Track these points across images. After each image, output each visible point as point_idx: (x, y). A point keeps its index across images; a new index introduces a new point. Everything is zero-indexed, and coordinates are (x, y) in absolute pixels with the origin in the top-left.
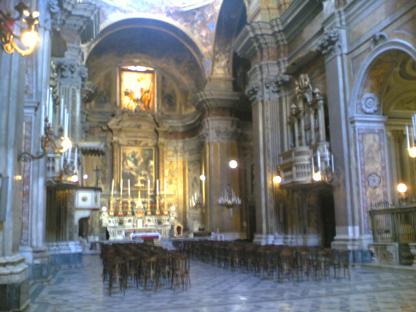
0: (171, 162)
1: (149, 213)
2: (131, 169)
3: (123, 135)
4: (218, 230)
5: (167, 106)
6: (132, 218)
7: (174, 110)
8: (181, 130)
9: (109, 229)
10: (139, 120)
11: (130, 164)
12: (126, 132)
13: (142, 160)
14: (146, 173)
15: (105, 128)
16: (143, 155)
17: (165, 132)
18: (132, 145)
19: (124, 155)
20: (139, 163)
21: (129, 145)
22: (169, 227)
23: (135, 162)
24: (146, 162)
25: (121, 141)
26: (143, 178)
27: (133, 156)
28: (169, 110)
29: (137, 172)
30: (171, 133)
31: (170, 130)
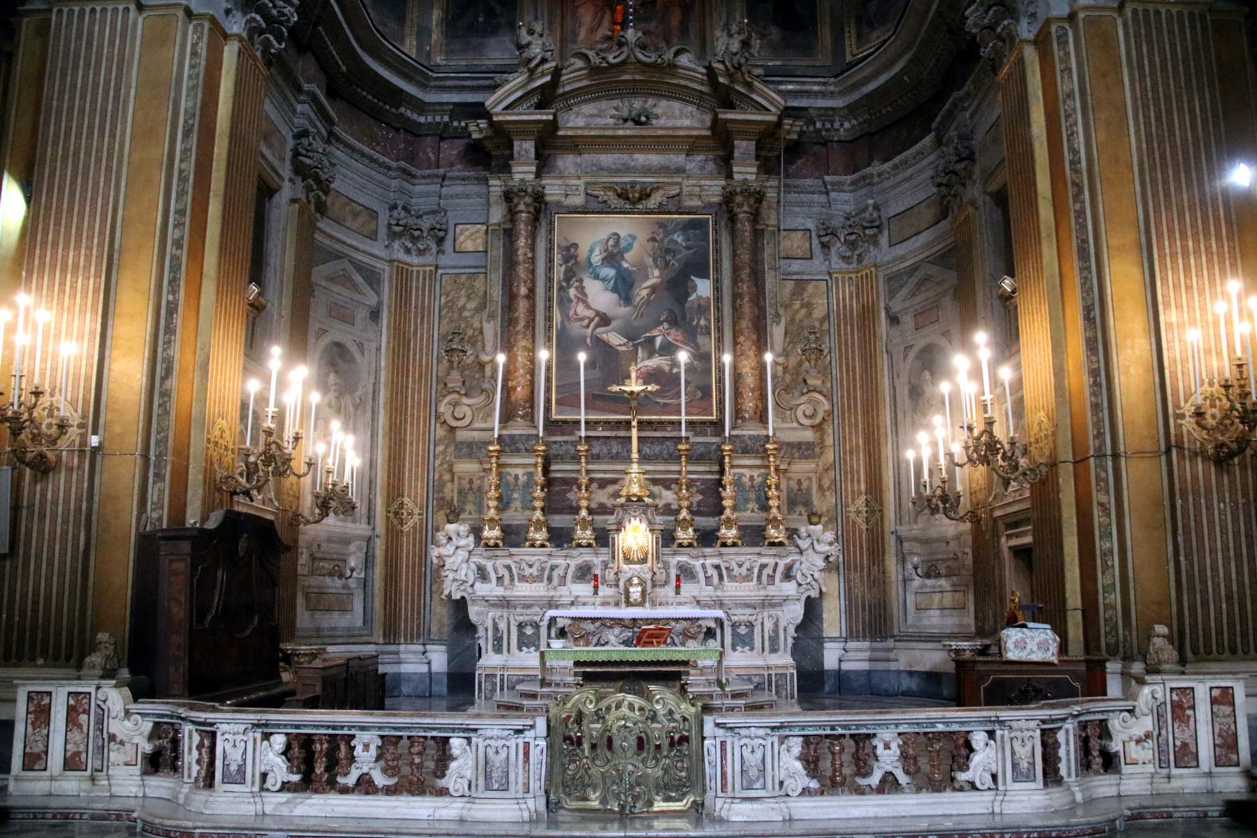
0: (801, 285)
1: (685, 535)
2: (605, 320)
3: (566, 162)
4: (1160, 643)
5: (775, 33)
6: (596, 559)
7: (807, 49)
8: (845, 128)
9: (474, 612)
10: (635, 89)
11: (600, 296)
12: (576, 145)
13: (655, 276)
14: (674, 336)
15: (477, 129)
16: (663, 254)
17: (766, 137)
18: (606, 209)
19: (570, 253)
20: (641, 293)
21: (595, 206)
22: (796, 612)
23: (624, 286)
24: (677, 286)
25: (553, 189)
26: (656, 362)
27: (612, 258)
28: (775, 49)
29: (630, 335)
30: (795, 150)
31: (792, 129)
